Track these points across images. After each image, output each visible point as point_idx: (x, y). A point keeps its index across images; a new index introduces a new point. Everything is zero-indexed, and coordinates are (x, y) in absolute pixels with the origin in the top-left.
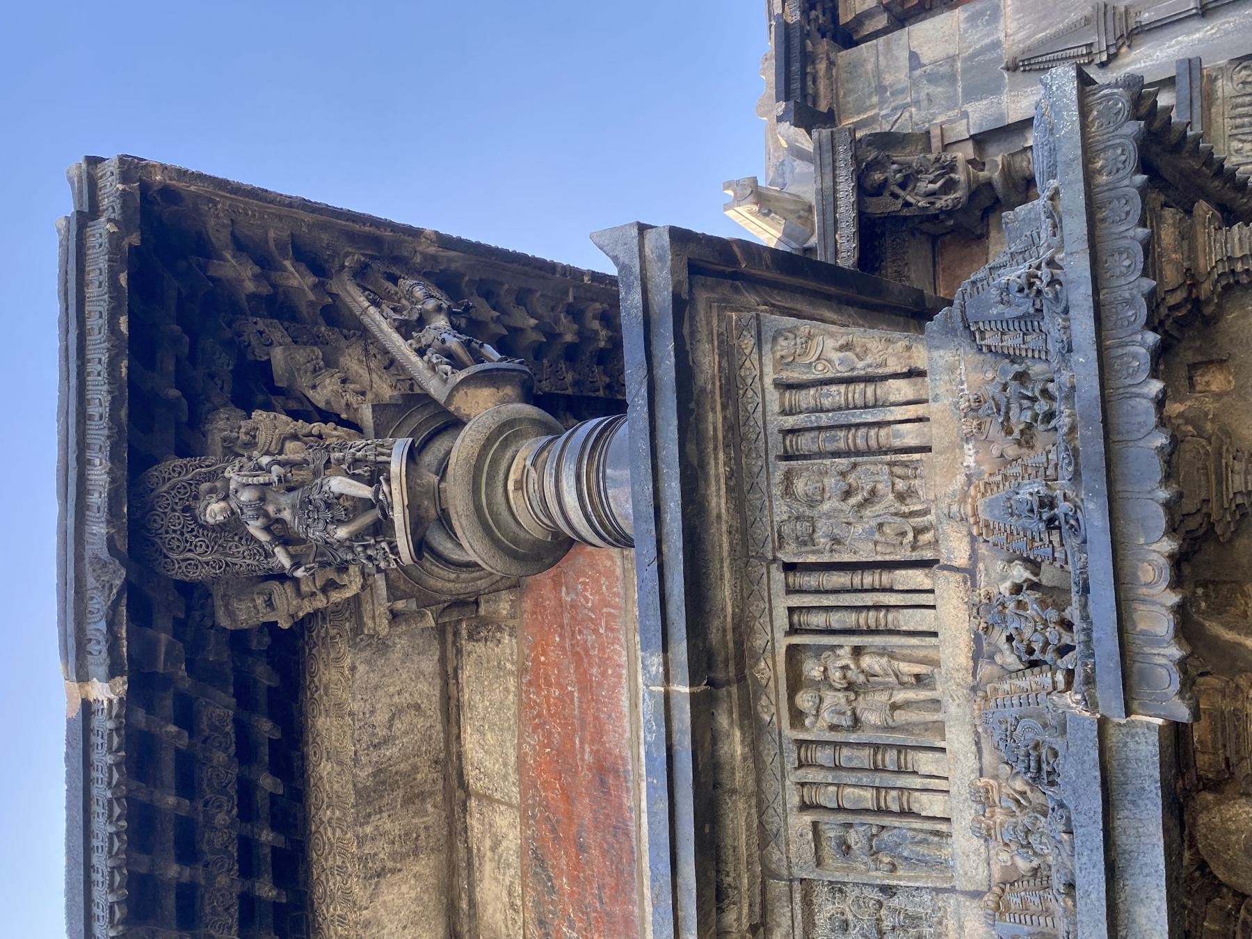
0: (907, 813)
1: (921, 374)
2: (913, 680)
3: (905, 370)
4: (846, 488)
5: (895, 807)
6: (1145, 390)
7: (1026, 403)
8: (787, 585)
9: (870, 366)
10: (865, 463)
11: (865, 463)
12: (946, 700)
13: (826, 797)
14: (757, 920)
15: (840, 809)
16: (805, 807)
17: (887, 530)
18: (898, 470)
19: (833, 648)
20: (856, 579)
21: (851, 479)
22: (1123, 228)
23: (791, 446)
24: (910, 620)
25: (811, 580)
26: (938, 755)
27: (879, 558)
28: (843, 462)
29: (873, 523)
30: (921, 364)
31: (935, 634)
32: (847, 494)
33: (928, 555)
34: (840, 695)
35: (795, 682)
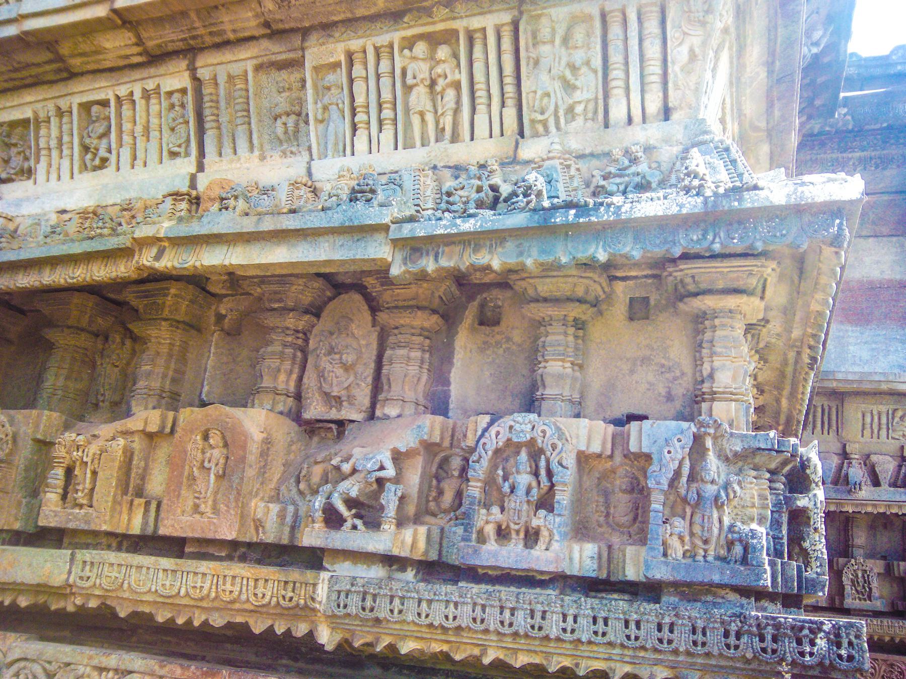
0: (354, 128)
1: (667, 119)
2: (441, 126)
3: (670, 105)
4: (577, 65)
5: (356, 120)
6: (600, 250)
7: (622, 188)
8: (503, 25)
9: (676, 76)
10: (597, 79)
11: (597, 79)
12: (427, 149)
13: (358, 71)
14: (274, 27)
15: (351, 81)
16: (350, 56)
17: (546, 100)
18: (591, 106)
19: (458, 65)
20: (509, 80)
21: (584, 69)
22: (722, 235)
23: (613, 17)
24: (481, 120)
25: (507, 44)
26: (392, 146)
27: (524, 95)
28: (597, 62)
29: (550, 90)
30: (675, 116)
31: (472, 139)
32: (573, 68)
33: (527, 132)
34: (427, 75)
35: (434, 40)
